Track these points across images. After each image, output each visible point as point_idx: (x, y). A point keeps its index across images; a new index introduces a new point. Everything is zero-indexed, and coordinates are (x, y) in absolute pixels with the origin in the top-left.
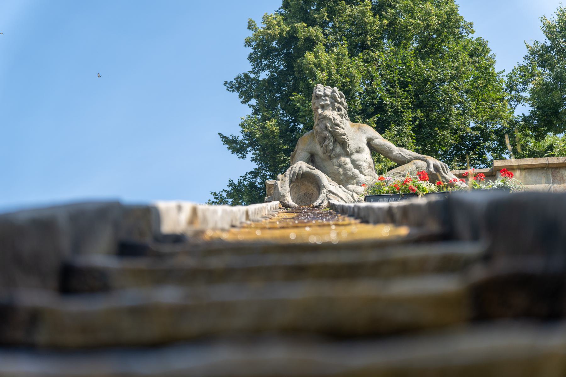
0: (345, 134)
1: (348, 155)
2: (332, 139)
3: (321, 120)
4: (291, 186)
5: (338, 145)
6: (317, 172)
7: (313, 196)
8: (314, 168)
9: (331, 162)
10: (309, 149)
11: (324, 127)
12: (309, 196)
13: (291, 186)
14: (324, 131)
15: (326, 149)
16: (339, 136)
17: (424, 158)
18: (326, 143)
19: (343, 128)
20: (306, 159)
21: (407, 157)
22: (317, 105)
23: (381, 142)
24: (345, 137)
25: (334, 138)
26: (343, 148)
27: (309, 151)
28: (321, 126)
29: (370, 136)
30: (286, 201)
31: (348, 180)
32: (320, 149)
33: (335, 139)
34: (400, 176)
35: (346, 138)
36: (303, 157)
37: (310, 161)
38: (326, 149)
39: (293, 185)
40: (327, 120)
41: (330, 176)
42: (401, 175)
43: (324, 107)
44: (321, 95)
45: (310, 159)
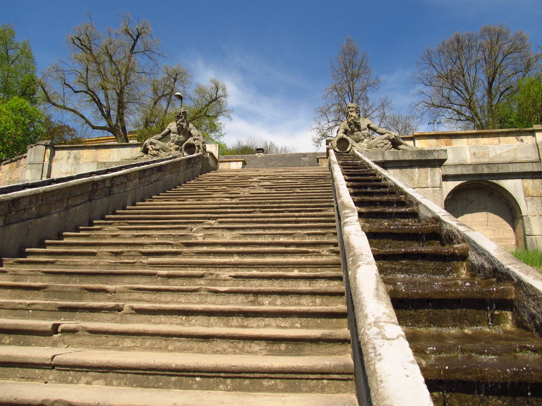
0: (359, 123)
1: (360, 131)
6: (348, 138)
18: (352, 126)
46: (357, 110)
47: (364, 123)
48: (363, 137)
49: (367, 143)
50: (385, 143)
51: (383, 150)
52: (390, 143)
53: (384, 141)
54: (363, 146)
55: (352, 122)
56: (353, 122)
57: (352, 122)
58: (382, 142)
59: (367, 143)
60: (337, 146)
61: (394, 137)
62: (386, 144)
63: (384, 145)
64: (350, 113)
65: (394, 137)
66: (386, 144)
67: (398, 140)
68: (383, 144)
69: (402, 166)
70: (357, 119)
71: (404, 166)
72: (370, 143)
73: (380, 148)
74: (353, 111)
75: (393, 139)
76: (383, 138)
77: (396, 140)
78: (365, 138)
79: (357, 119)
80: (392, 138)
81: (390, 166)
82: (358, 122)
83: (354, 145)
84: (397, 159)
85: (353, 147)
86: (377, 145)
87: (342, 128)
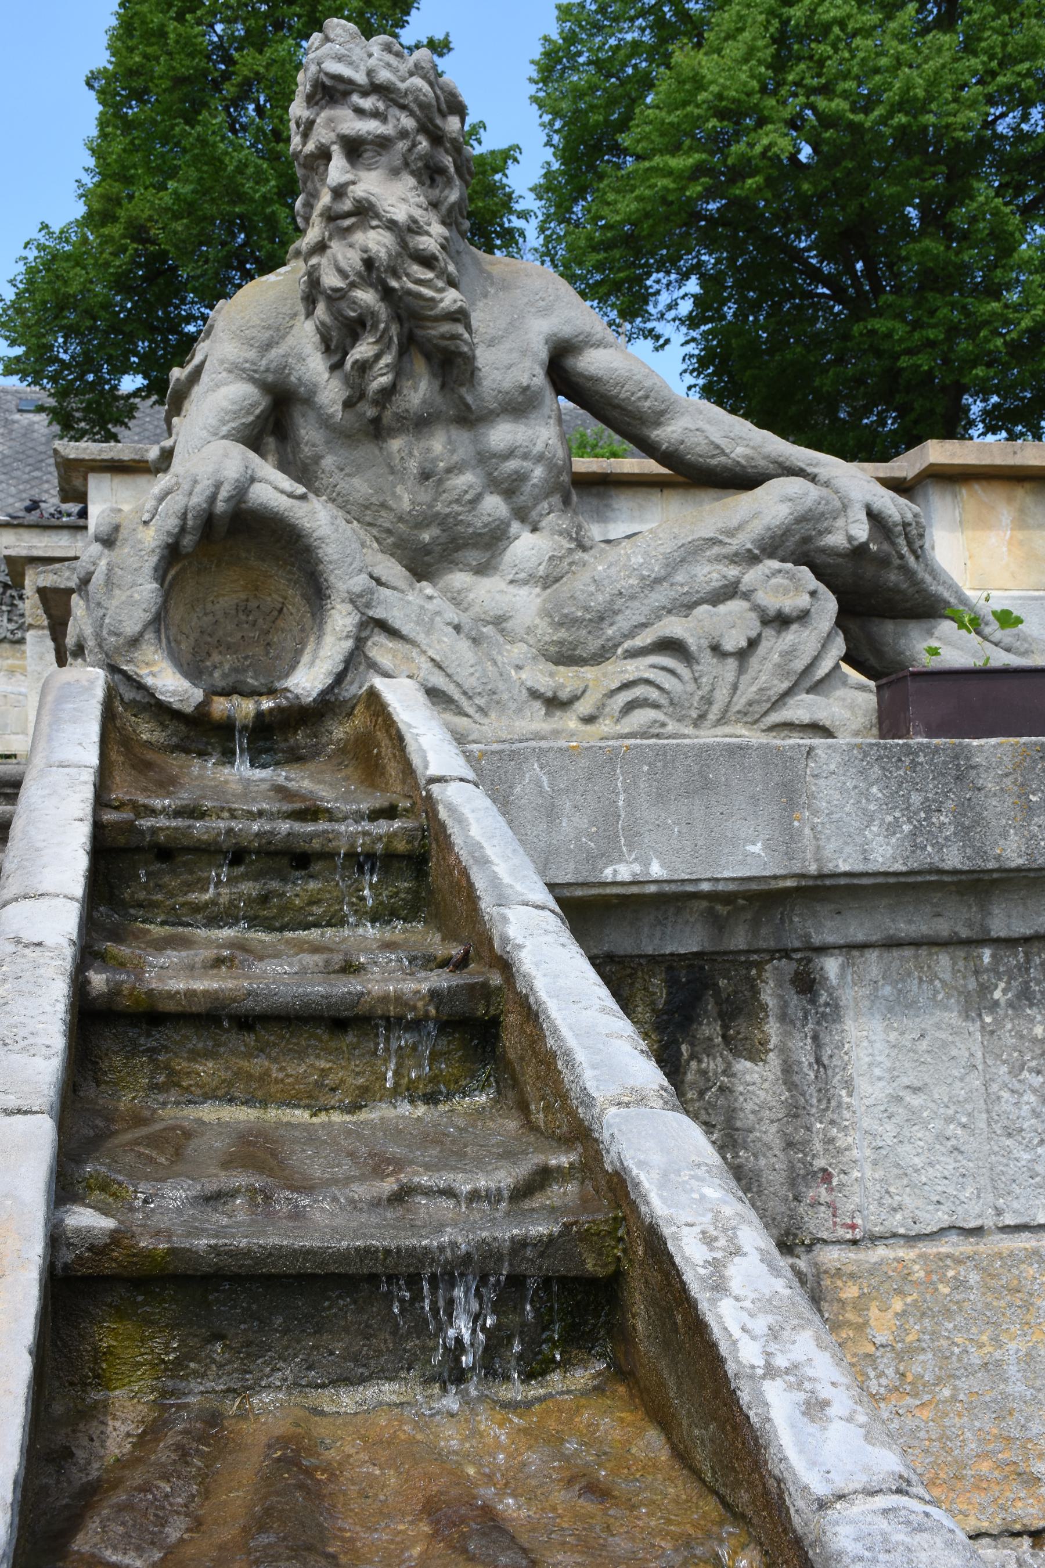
0: (460, 316)
2: (394, 330)
3: (347, 222)
4: (172, 573)
5: (420, 366)
7: (280, 623)
8: (301, 490)
9: (377, 452)
10: (267, 370)
11: (359, 266)
12: (260, 621)
13: (172, 573)
14: (353, 285)
15: (357, 381)
16: (429, 324)
17: (816, 465)
18: (363, 350)
19: (452, 283)
20: (251, 418)
21: (739, 453)
22: (322, 134)
23: (614, 365)
24: (460, 329)
25: (401, 325)
26: (443, 386)
27: (270, 378)
28: (340, 257)
29: (566, 331)
30: (142, 672)
31: (457, 549)
32: (326, 375)
33: (406, 330)
34: (718, 559)
35: (466, 336)
36: (235, 407)
37: (270, 426)
38: (357, 381)
39: (183, 570)
40: (373, 228)
41: (368, 519)
42: (724, 550)
43: (360, 156)
44: (350, 82)
45: (272, 420)
46: (437, 138)
47: (513, 326)
48: (494, 505)
49: (548, 581)
50: (773, 601)
51: (748, 692)
52: (829, 605)
53: (752, 576)
54: (499, 621)
55: (366, 296)
56: (387, 294)
57: (366, 296)
58: (729, 592)
59: (548, 581)
60: (158, 621)
61: (861, 531)
62: (781, 621)
63: (752, 626)
64: (337, 170)
65: (861, 531)
66: (781, 621)
67: (904, 569)
68: (735, 606)
69: (999, 927)
70: (427, 261)
71: (1021, 929)
72: (579, 584)
73: (707, 662)
74: (383, 143)
75: (859, 551)
76: (744, 541)
77: (884, 562)
78: (521, 514)
79: (427, 261)
80: (836, 540)
81: (860, 937)
82: (450, 299)
83: (396, 618)
84: (953, 859)
85: (381, 648)
86: (674, 627)
87: (238, 371)
